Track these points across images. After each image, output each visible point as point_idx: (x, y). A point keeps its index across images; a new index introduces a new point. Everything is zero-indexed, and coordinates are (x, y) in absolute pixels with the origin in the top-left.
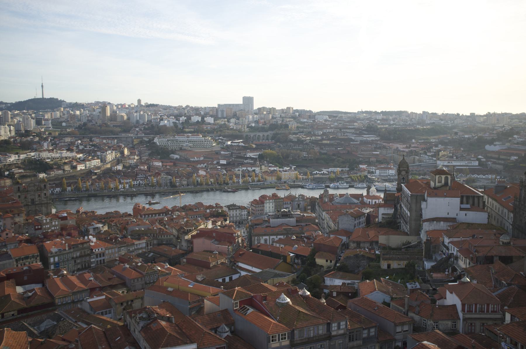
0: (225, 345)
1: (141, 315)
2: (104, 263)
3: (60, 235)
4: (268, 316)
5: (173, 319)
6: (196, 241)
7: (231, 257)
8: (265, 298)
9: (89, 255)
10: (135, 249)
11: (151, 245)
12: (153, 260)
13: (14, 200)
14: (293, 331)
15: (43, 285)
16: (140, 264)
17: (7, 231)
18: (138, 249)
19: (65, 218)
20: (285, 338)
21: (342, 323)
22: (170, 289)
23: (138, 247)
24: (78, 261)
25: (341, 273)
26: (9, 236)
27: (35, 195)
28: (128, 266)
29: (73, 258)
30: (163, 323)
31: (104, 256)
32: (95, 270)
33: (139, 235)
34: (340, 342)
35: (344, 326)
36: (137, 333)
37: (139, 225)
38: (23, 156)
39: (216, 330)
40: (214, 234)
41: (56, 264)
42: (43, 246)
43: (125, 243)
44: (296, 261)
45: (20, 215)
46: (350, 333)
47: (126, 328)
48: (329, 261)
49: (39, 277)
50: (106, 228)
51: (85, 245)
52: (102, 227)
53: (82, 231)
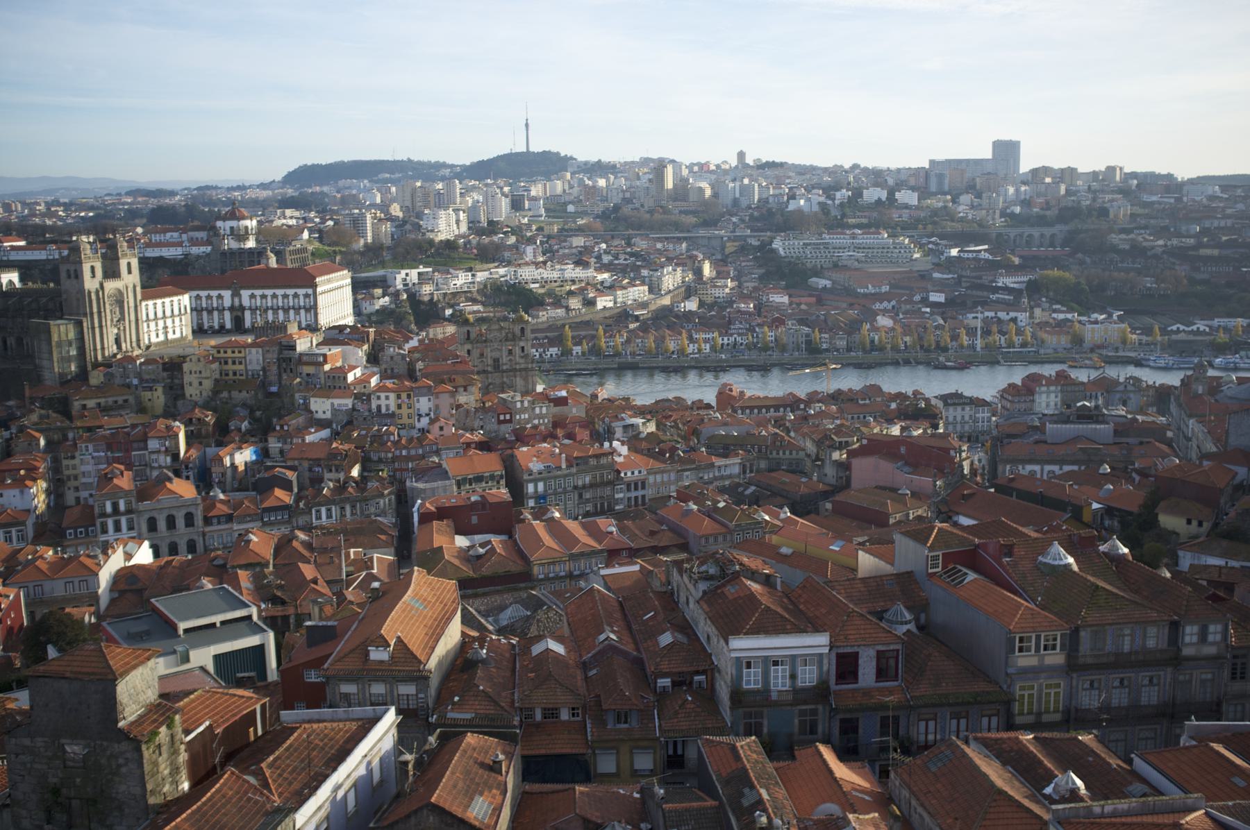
0: (899, 647)
1: (703, 568)
2: (644, 503)
3: (550, 436)
4: (1015, 592)
5: (779, 581)
6: (856, 463)
7: (941, 501)
8: (1009, 550)
9: (611, 483)
10: (716, 479)
11: (751, 471)
12: (756, 501)
13: (457, 357)
14: (1076, 631)
15: (511, 537)
16: (721, 505)
17: (442, 422)
18: (722, 478)
19: (561, 402)
20: (1054, 648)
21: (1212, 628)
22: (784, 550)
23: (723, 472)
24: (587, 495)
25: (1225, 543)
26: (445, 432)
27: (500, 350)
28: (695, 507)
29: (575, 487)
30: (755, 587)
31: (643, 488)
32: (620, 517)
33: (726, 447)
34: (1204, 676)
35: (1218, 637)
36: (691, 605)
37: (726, 424)
38: (481, 276)
39: (880, 615)
40: (903, 450)
41: (539, 498)
42: (512, 456)
43: (693, 462)
44: (1107, 523)
45: (469, 388)
46: (1235, 657)
47: (669, 600)
48: (1195, 523)
49: (500, 519)
50: (651, 427)
51: (603, 461)
52: (644, 424)
53: (598, 433)
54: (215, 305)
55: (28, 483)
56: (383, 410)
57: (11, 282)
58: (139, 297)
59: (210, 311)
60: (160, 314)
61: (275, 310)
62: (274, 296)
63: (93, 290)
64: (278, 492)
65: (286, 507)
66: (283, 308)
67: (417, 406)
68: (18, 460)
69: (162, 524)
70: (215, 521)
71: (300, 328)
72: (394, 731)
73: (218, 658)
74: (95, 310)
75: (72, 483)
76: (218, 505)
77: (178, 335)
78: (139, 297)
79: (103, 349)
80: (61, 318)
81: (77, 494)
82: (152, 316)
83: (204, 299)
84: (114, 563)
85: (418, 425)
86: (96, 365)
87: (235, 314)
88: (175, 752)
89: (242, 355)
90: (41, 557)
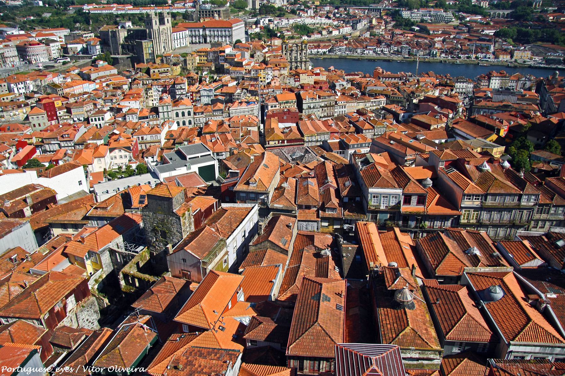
15: (297, 125)
19: (317, 74)
29: (321, 107)
38: (291, 21)
40: (439, 102)
48: (540, 140)
60: (178, 38)
64: (219, 104)
65: (222, 110)
68: (133, 91)
69: (180, 115)
72: (257, 212)
73: (199, 168)
74: (157, 36)
75: (151, 98)
77: (185, 45)
82: (176, 38)
84: (166, 129)
86: (157, 56)
88: (191, 218)
90: (143, 127)
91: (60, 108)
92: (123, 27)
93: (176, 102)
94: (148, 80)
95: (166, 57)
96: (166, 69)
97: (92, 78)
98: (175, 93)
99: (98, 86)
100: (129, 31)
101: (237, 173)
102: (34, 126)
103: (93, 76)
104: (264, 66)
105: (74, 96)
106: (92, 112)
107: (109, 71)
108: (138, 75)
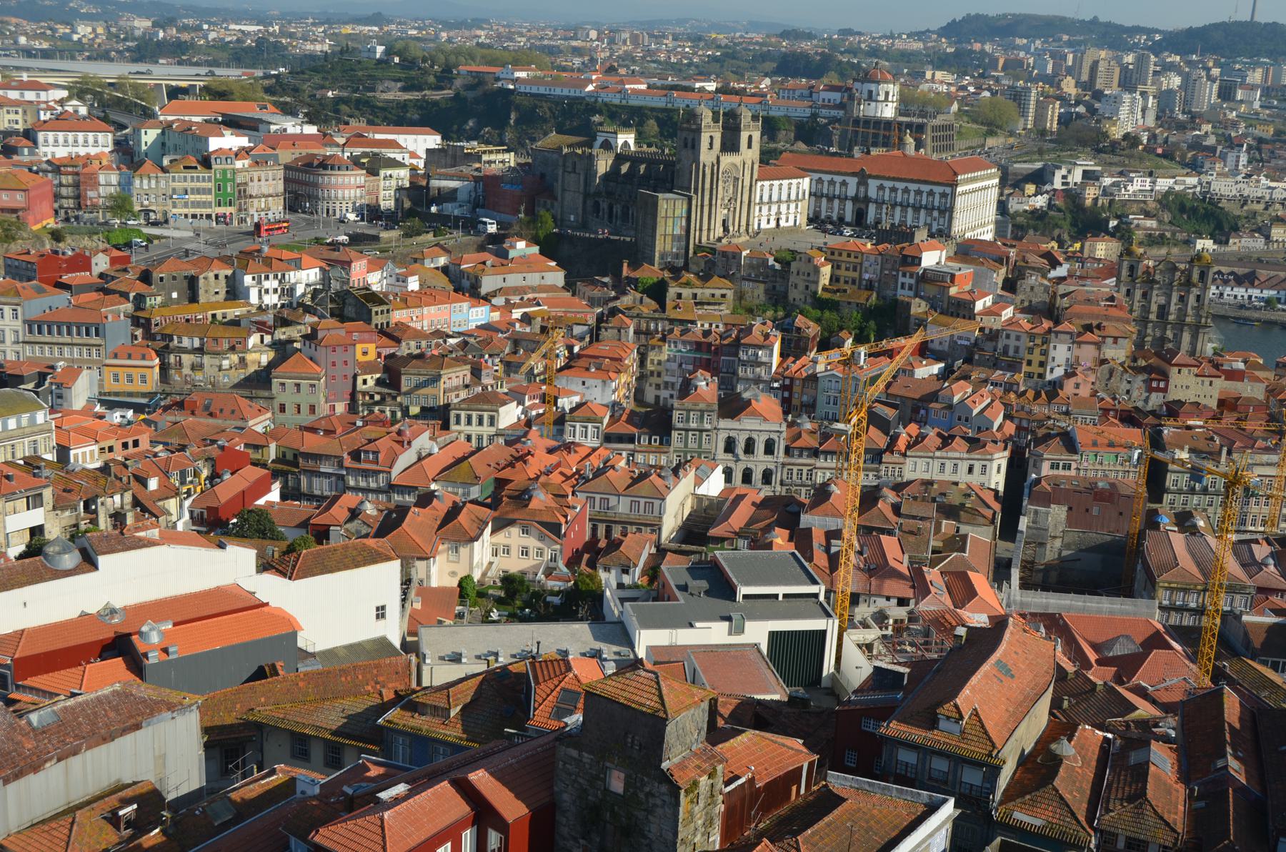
17: (1079, 379)
19: (1233, 375)
54: (837, 193)
55: (611, 374)
56: (1011, 353)
57: (626, 143)
58: (755, 176)
59: (830, 199)
60: (775, 198)
61: (904, 206)
62: (906, 191)
63: (709, 164)
66: (913, 206)
67: (1052, 353)
68: (602, 348)
70: (796, 453)
71: (931, 235)
74: (707, 186)
75: (654, 380)
76: (804, 435)
77: (791, 223)
78: (755, 176)
79: (709, 229)
80: (670, 191)
81: (658, 393)
82: (766, 199)
83: (826, 184)
85: (1049, 377)
86: (699, 248)
87: (858, 205)
89: (858, 260)
91: (368, 368)
92: (607, 146)
93: (732, 406)
94: (655, 319)
95: (724, 254)
96: (718, 293)
97: (484, 290)
98: (735, 373)
99: (496, 316)
100: (620, 159)
101: (903, 674)
102: (283, 408)
103: (489, 283)
104: (1047, 324)
105: (419, 335)
106: (463, 394)
107: (537, 276)
108: (626, 300)
